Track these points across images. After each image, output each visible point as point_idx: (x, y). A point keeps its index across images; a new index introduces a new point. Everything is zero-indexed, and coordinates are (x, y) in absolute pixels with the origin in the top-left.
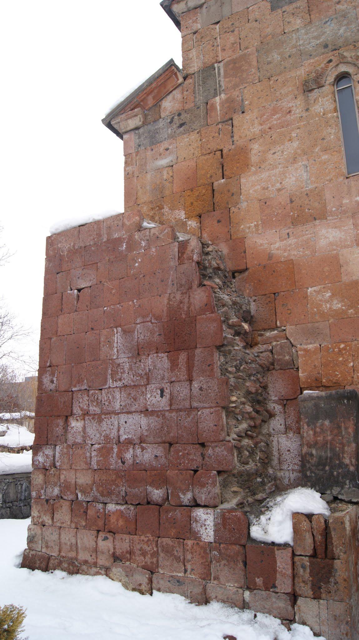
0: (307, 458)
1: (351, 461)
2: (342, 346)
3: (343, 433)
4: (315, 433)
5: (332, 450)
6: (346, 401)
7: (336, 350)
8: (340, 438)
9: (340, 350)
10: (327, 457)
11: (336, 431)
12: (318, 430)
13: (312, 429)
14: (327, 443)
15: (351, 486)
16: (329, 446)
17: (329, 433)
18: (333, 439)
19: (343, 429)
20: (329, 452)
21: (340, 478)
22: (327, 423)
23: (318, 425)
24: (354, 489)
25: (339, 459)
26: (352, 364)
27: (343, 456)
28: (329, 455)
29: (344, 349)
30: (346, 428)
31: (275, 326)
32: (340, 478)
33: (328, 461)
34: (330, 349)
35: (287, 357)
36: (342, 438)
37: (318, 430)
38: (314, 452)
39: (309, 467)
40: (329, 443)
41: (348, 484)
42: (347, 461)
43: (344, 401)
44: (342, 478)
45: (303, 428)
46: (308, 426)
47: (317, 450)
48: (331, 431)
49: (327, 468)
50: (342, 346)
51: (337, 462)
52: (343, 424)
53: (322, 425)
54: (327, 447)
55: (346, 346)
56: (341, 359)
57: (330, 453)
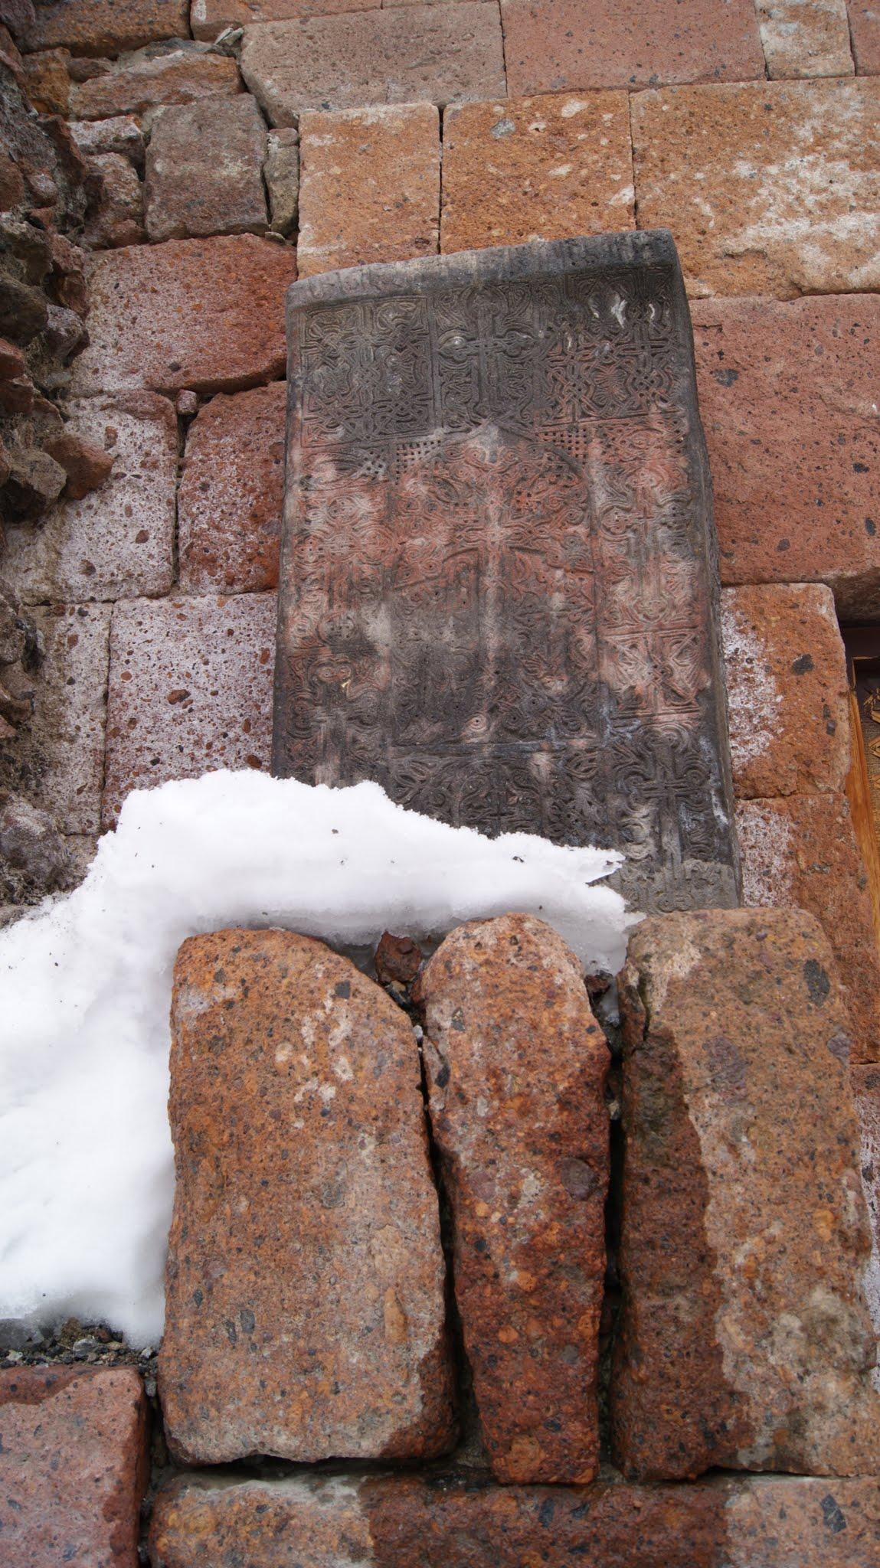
0: (324, 673)
1: (665, 673)
2: (573, 107)
3: (601, 499)
4: (393, 512)
5: (520, 609)
6: (618, 309)
7: (538, 126)
8: (582, 530)
9: (559, 130)
10: (476, 663)
11: (545, 491)
12: (414, 487)
13: (371, 485)
14: (479, 570)
15: (672, 843)
16: (491, 582)
17: (493, 502)
18: (523, 544)
19: (596, 474)
20: (489, 621)
21: (583, 792)
22: (483, 443)
23: (417, 457)
24: (690, 864)
25: (570, 664)
26: (627, 195)
27: (599, 643)
28: (493, 642)
29: (588, 122)
30: (617, 470)
31: (180, 25)
32: (583, 792)
33: (488, 680)
34: (502, 120)
35: (233, 170)
36: (592, 532)
37: (414, 487)
38: (379, 628)
39: (335, 735)
40: (493, 566)
41: (644, 830)
42: (631, 673)
43: (604, 308)
44: (598, 796)
45: (305, 484)
46: (344, 465)
47: (398, 615)
48: (510, 494)
49: (478, 729)
50: (573, 107)
51: (558, 686)
52: (596, 450)
53: (450, 454)
54: (478, 590)
55: (595, 109)
56: (563, 170)
57: (503, 629)
